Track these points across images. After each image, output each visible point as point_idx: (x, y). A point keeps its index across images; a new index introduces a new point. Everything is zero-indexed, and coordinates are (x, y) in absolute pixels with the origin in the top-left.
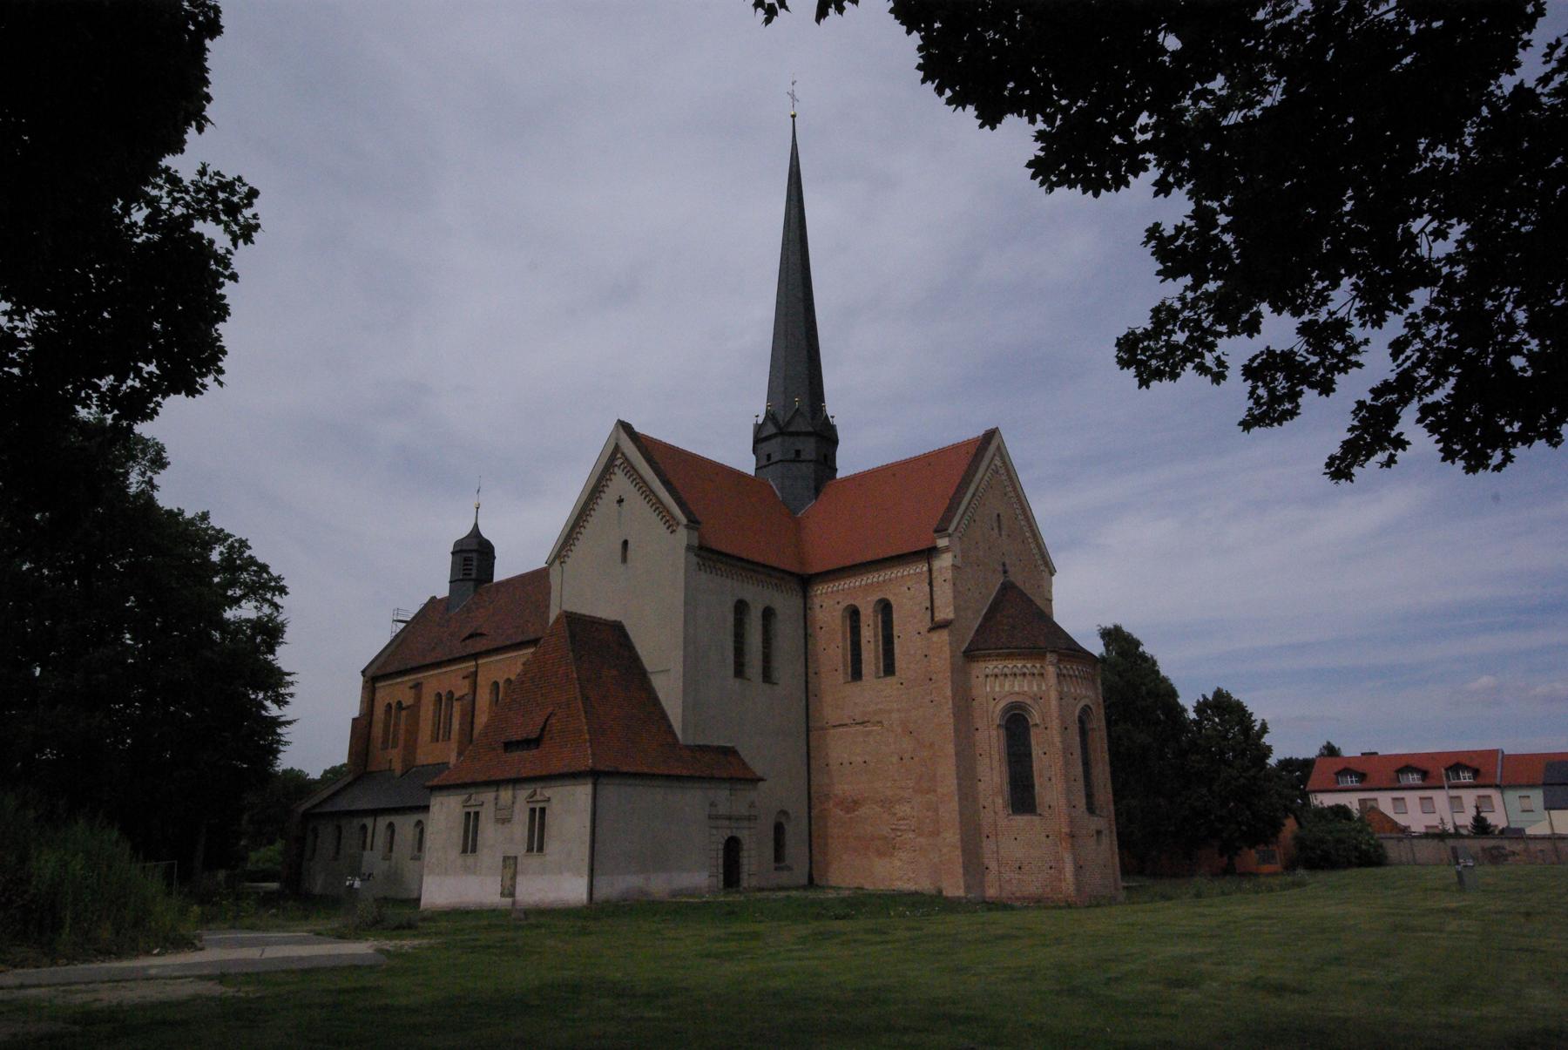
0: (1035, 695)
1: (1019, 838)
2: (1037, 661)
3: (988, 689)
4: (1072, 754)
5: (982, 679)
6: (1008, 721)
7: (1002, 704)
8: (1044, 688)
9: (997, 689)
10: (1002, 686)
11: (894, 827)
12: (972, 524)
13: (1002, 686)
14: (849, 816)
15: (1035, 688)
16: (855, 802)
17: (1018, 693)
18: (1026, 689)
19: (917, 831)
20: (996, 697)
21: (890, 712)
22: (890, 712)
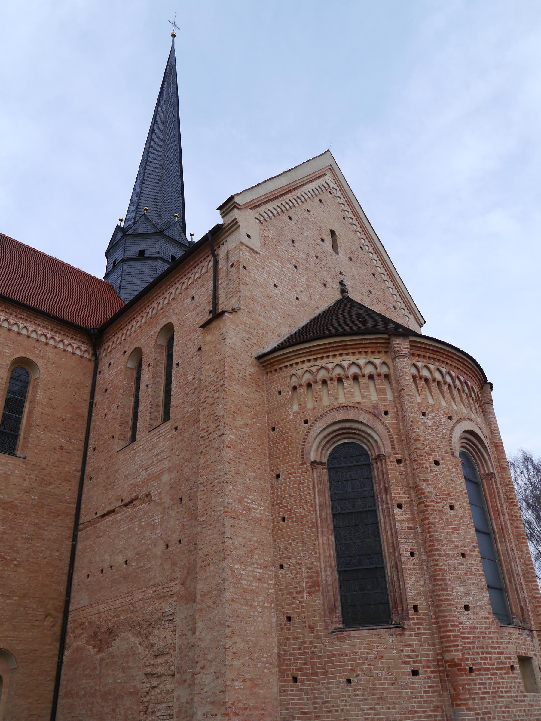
0: (375, 407)
1: (355, 680)
2: (376, 355)
3: (296, 408)
4: (452, 508)
5: (287, 392)
6: (331, 457)
7: (320, 425)
8: (389, 396)
9: (310, 405)
10: (317, 399)
11: (148, 670)
12: (285, 217)
13: (317, 399)
14: (100, 655)
15: (374, 398)
16: (110, 631)
17: (345, 407)
18: (358, 399)
19: (177, 676)
20: (308, 418)
21: (157, 477)
22: (157, 477)
